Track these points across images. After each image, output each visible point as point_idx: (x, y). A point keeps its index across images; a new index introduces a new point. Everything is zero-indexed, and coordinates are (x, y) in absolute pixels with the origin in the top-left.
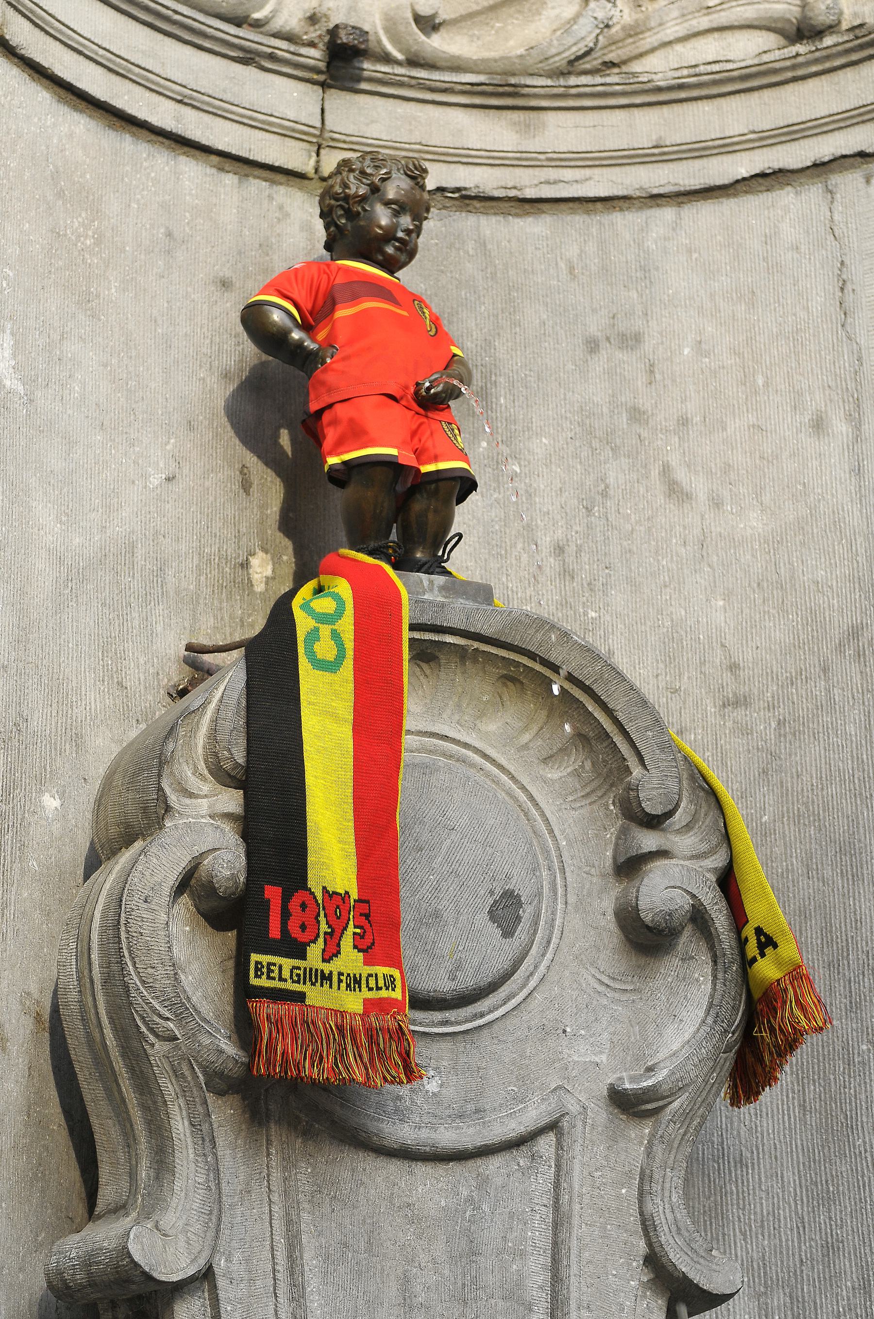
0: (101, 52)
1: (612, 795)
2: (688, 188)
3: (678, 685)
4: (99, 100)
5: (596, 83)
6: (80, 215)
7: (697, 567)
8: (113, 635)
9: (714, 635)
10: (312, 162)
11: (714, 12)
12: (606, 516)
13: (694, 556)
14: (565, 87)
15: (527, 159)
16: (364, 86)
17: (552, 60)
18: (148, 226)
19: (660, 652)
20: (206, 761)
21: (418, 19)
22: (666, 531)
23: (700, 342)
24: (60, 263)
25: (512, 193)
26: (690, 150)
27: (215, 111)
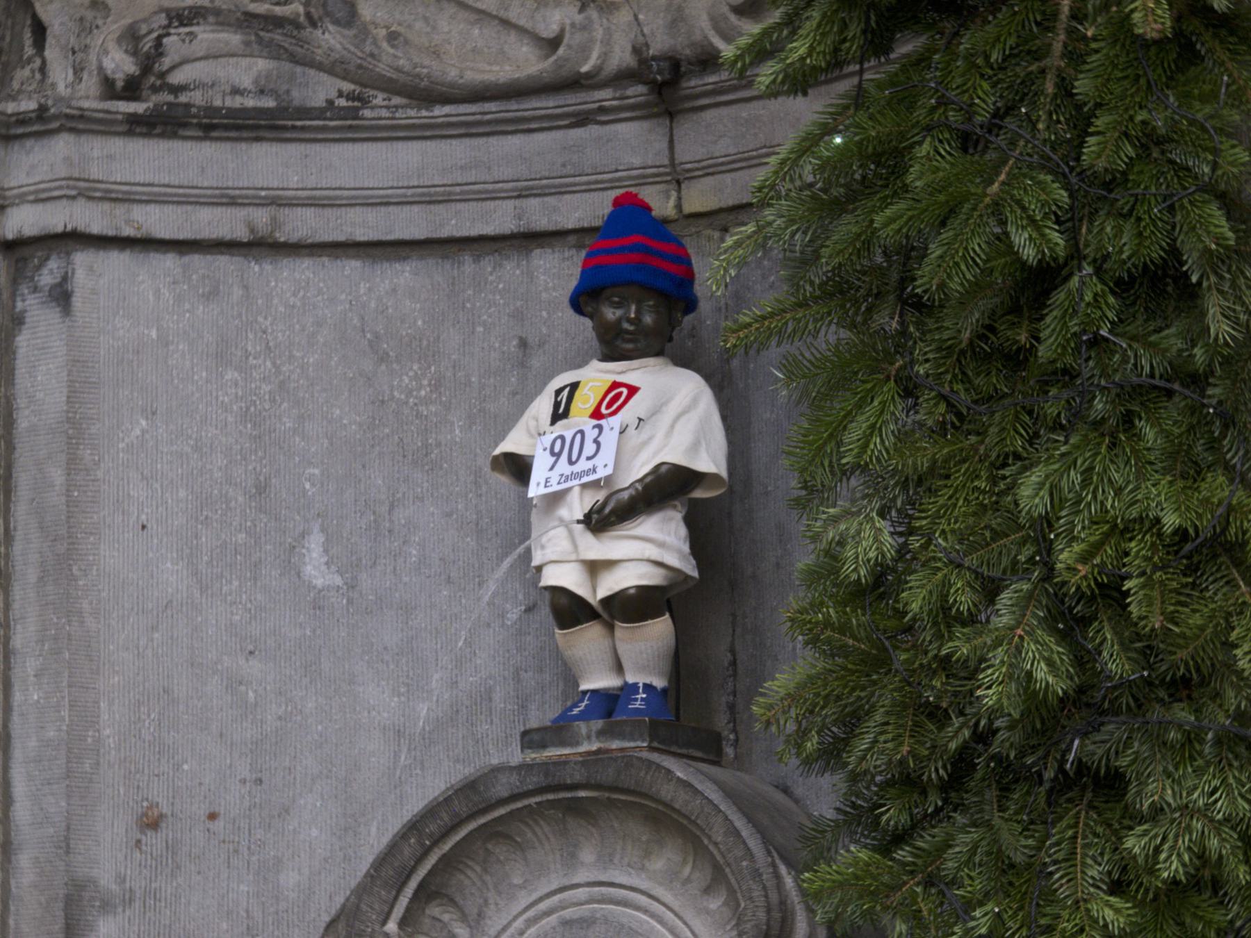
0: (410, 192)
6: (411, 369)
10: (672, 202)
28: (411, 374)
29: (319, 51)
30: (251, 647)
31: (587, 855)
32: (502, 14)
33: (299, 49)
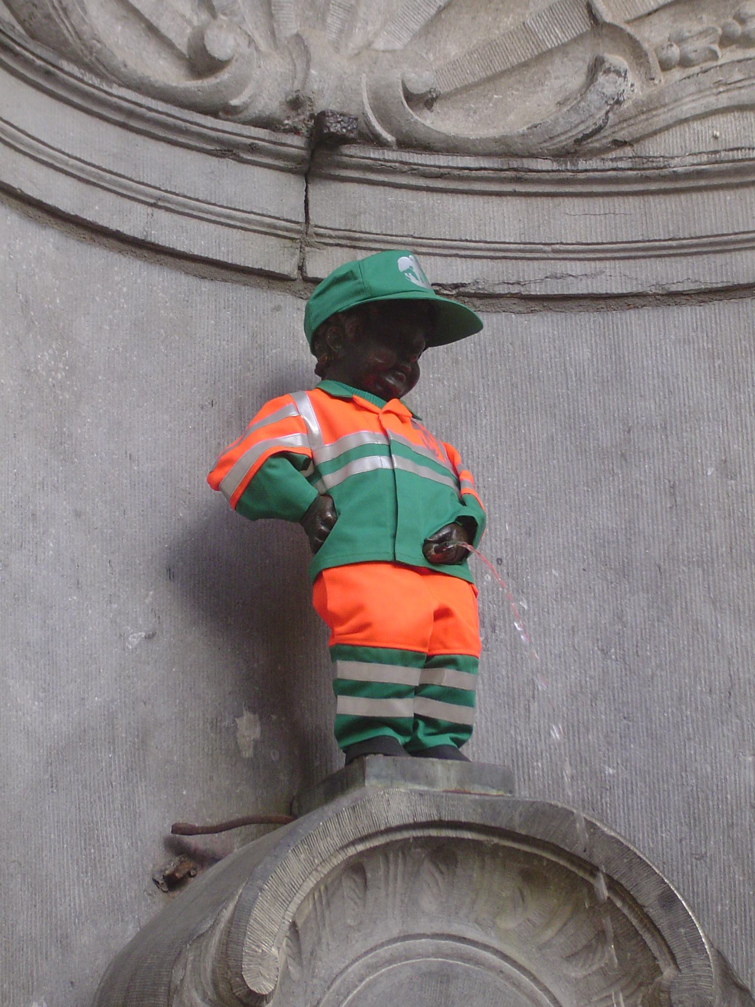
0: (72, 162)
1: (641, 995)
2: (709, 286)
3: (703, 851)
4: (69, 215)
5: (607, 167)
6: (50, 347)
7: (724, 718)
8: (95, 819)
9: (742, 795)
10: (295, 260)
11: (734, 89)
12: (624, 660)
13: (721, 705)
14: (573, 171)
15: (532, 251)
17: (558, 139)
18: (121, 349)
19: (684, 813)
20: (215, 985)
21: (410, 97)
22: (690, 677)
23: (725, 461)
24: (32, 404)
25: (515, 290)
26: (711, 244)
27: (190, 212)
28: (50, 351)
31: (428, 902)
32: (154, 20)
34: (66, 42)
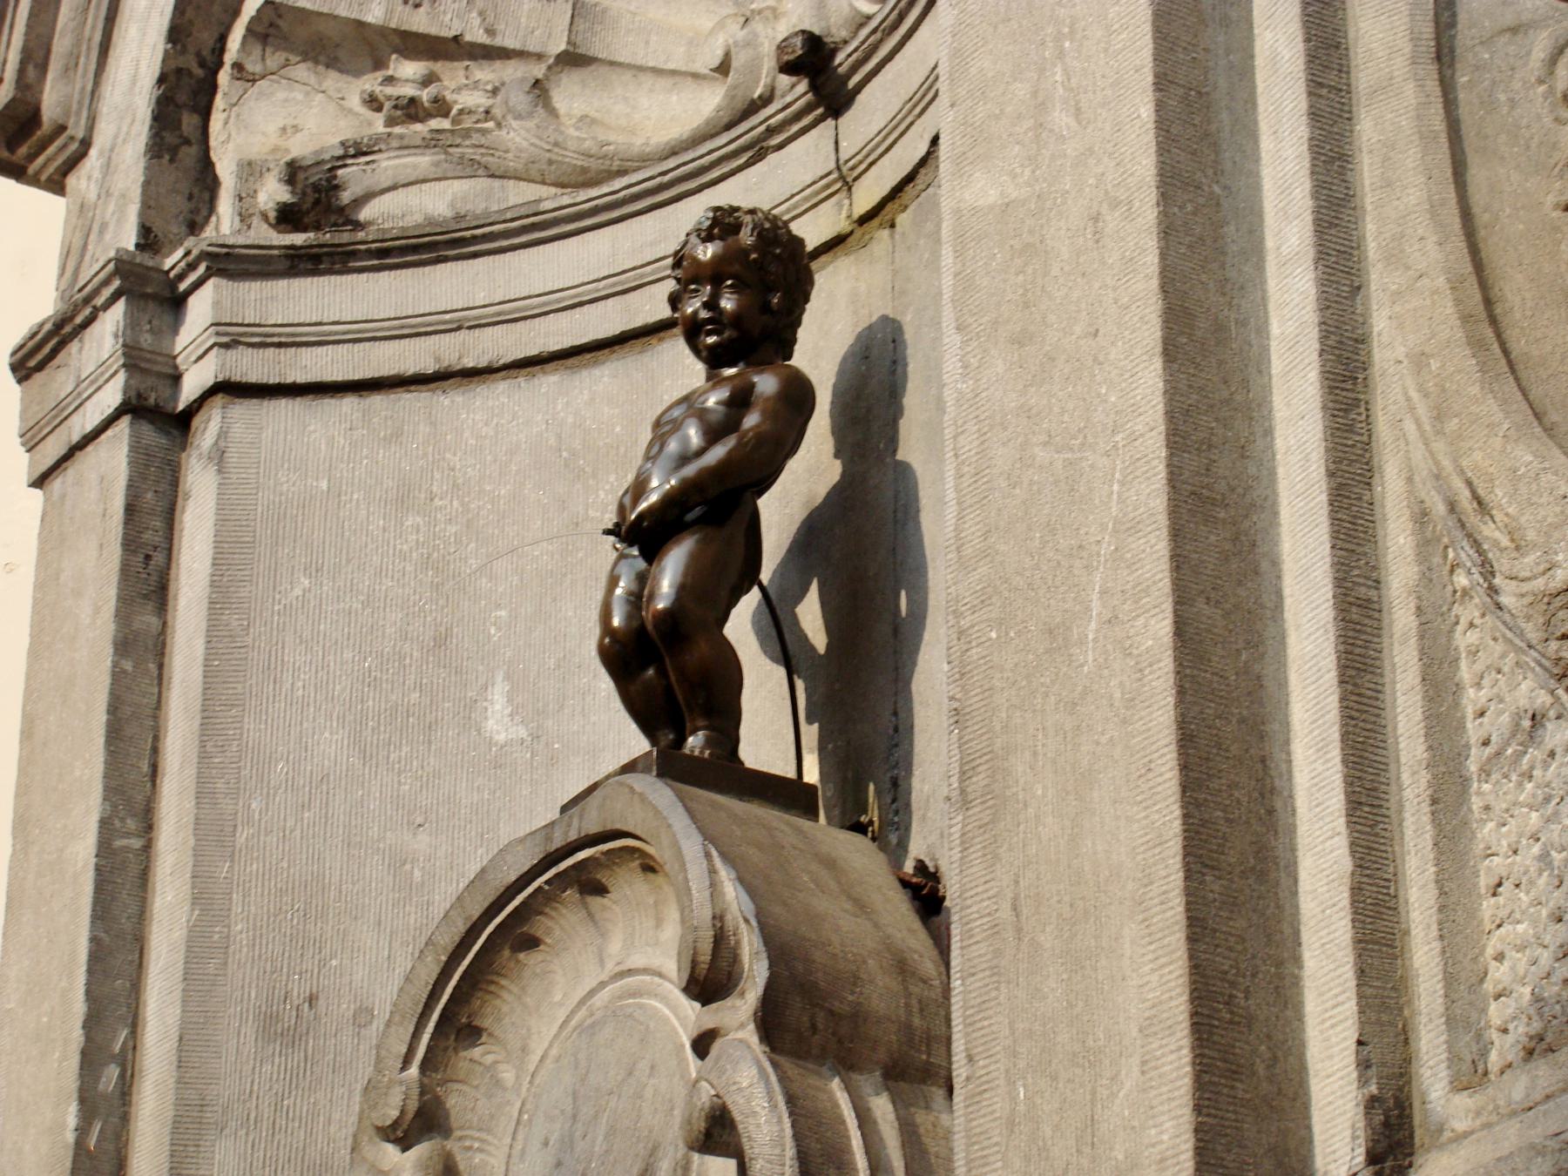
16: (852, 83)
29: (510, 156)
30: (419, 820)
31: (615, 947)
33: (490, 159)
34: (584, 170)
